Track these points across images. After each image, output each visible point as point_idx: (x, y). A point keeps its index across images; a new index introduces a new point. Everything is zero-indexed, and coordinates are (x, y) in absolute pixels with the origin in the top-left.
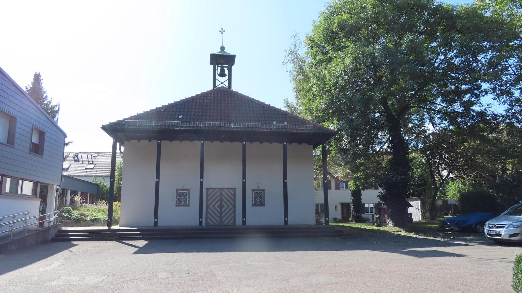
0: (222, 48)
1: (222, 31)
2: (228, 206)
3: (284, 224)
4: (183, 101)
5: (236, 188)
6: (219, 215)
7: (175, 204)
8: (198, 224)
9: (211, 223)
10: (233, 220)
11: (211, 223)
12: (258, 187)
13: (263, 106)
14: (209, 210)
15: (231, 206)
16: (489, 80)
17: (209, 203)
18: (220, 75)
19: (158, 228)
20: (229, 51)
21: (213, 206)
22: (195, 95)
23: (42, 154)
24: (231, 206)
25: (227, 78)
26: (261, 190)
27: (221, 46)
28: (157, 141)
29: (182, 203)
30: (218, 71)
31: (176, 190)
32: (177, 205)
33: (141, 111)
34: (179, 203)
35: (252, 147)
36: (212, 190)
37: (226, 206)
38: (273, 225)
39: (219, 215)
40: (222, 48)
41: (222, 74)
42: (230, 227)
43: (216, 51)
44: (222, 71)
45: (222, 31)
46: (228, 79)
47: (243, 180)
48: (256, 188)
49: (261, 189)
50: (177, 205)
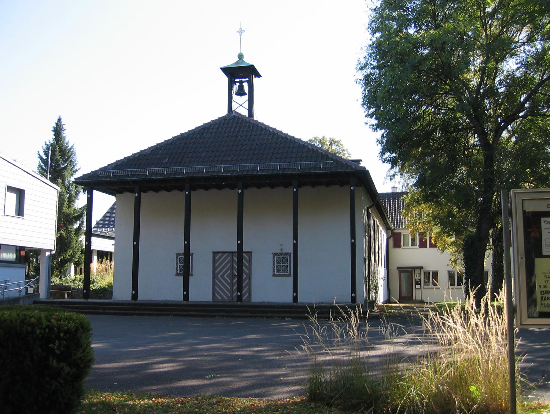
0: (241, 56)
1: (240, 32)
2: (222, 276)
3: (132, 299)
4: (176, 138)
5: (252, 252)
6: (229, 288)
7: (175, 273)
8: (292, 301)
9: (220, 298)
10: (247, 294)
11: (220, 298)
12: (281, 250)
13: (278, 136)
14: (216, 281)
15: (219, 276)
16: (484, 68)
17: (216, 272)
18: (237, 94)
19: (137, 302)
20: (248, 60)
21: (222, 276)
22: (194, 128)
23: (23, 216)
24: (219, 276)
25: (246, 98)
26: (285, 253)
27: (239, 54)
28: (134, 194)
29: (281, 272)
30: (235, 88)
31: (273, 254)
32: (274, 275)
33: (121, 157)
34: (276, 272)
35: (305, 192)
36: (220, 254)
37: (225, 276)
38: (145, 300)
39: (229, 288)
40: (241, 56)
41: (241, 93)
42: (220, 303)
43: (231, 61)
44: (241, 88)
45: (240, 32)
46: (247, 99)
47: (355, 241)
48: (278, 251)
49: (285, 252)
50: (274, 275)
